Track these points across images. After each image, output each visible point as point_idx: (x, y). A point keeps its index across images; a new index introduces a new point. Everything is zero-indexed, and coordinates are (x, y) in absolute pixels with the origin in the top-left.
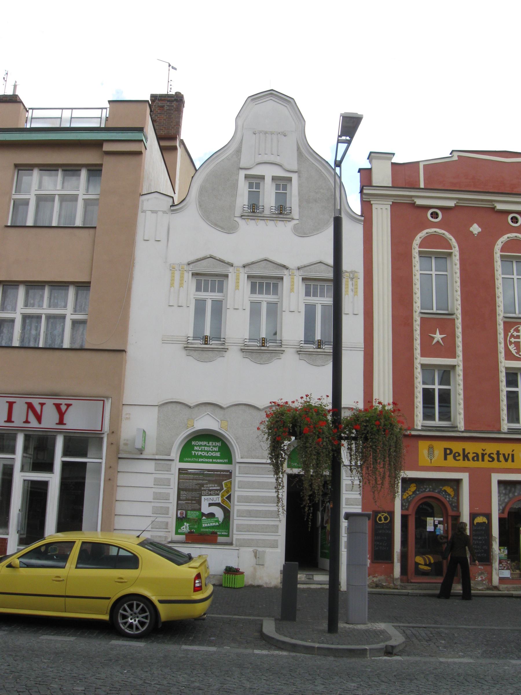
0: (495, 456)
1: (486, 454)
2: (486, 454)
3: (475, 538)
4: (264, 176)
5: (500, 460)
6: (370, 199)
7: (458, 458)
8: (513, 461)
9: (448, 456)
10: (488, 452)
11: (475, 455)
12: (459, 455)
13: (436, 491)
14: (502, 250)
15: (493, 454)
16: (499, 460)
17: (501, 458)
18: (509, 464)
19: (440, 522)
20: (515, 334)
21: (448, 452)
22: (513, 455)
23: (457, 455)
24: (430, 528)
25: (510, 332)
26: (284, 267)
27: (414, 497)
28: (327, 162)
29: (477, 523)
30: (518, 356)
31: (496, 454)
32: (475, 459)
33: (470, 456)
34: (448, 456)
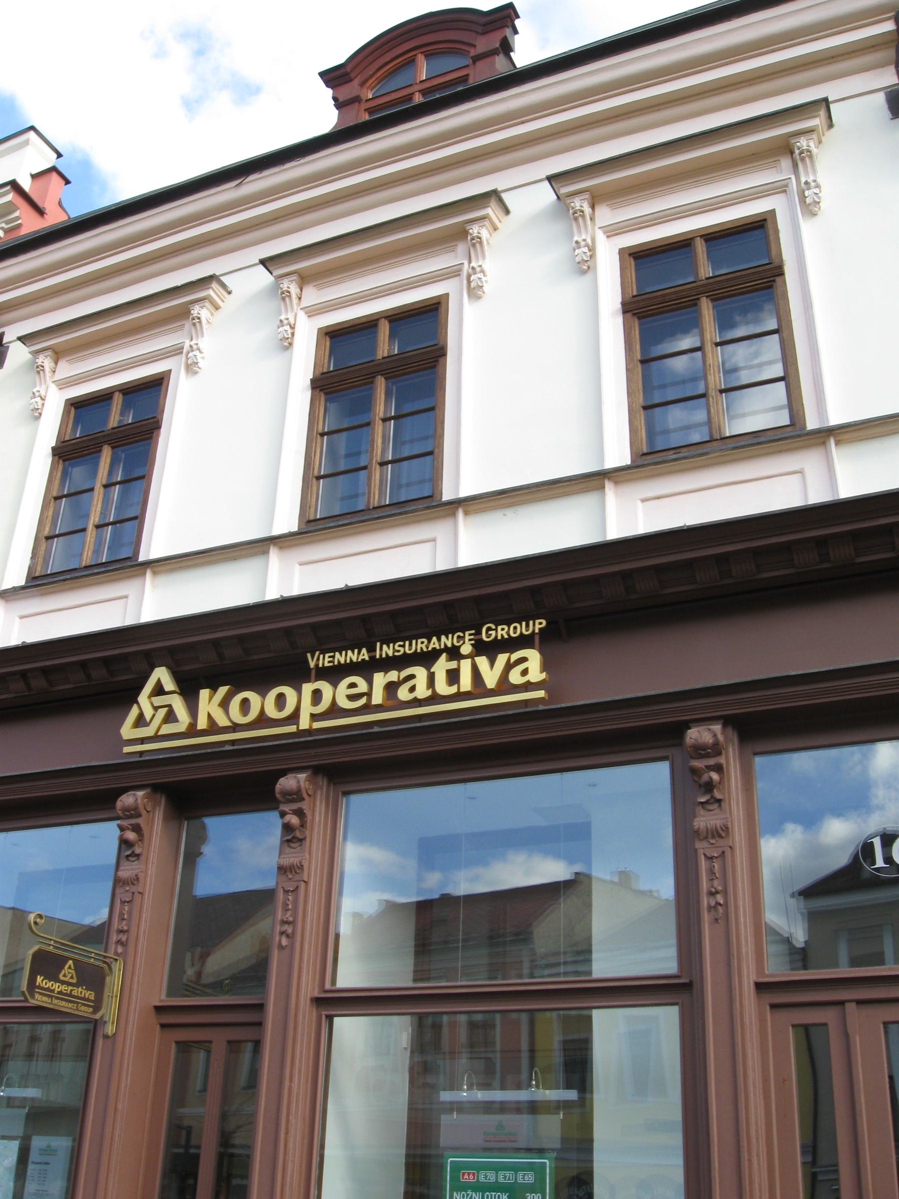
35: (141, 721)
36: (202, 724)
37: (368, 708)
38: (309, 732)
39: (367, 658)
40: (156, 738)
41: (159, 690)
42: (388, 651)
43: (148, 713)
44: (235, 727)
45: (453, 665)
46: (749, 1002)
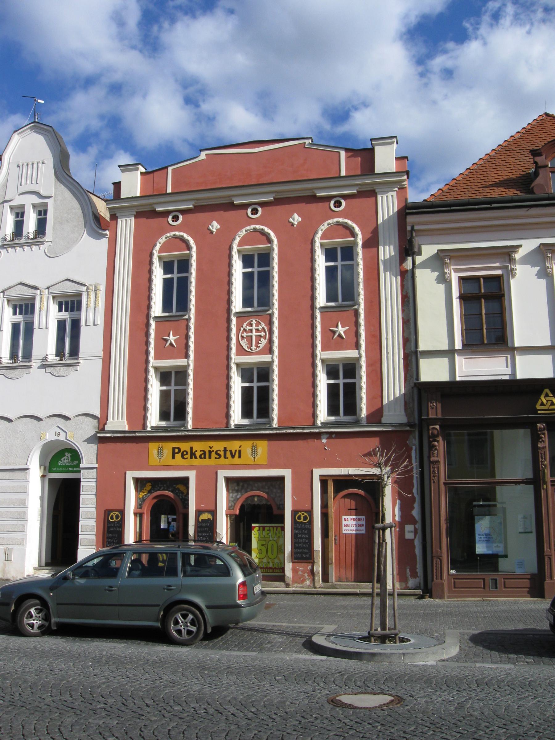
0: (222, 453)
1: (213, 451)
2: (213, 451)
3: (200, 534)
4: (25, 205)
5: (227, 456)
6: (116, 212)
7: (185, 457)
8: (240, 457)
9: (176, 455)
10: (215, 449)
11: (202, 452)
12: (187, 453)
13: (170, 490)
14: (240, 244)
15: (220, 451)
16: (225, 457)
17: (228, 454)
18: (236, 460)
19: (174, 520)
20: (248, 328)
21: (177, 450)
22: (240, 451)
23: (185, 453)
24: (163, 526)
25: (242, 327)
26: (36, 288)
27: (149, 496)
28: (78, 183)
29: (202, 520)
30: (250, 350)
31: (223, 451)
32: (203, 456)
33: (198, 454)
34: (176, 455)
35: (542, 404)
41: (547, 395)
43: (545, 401)
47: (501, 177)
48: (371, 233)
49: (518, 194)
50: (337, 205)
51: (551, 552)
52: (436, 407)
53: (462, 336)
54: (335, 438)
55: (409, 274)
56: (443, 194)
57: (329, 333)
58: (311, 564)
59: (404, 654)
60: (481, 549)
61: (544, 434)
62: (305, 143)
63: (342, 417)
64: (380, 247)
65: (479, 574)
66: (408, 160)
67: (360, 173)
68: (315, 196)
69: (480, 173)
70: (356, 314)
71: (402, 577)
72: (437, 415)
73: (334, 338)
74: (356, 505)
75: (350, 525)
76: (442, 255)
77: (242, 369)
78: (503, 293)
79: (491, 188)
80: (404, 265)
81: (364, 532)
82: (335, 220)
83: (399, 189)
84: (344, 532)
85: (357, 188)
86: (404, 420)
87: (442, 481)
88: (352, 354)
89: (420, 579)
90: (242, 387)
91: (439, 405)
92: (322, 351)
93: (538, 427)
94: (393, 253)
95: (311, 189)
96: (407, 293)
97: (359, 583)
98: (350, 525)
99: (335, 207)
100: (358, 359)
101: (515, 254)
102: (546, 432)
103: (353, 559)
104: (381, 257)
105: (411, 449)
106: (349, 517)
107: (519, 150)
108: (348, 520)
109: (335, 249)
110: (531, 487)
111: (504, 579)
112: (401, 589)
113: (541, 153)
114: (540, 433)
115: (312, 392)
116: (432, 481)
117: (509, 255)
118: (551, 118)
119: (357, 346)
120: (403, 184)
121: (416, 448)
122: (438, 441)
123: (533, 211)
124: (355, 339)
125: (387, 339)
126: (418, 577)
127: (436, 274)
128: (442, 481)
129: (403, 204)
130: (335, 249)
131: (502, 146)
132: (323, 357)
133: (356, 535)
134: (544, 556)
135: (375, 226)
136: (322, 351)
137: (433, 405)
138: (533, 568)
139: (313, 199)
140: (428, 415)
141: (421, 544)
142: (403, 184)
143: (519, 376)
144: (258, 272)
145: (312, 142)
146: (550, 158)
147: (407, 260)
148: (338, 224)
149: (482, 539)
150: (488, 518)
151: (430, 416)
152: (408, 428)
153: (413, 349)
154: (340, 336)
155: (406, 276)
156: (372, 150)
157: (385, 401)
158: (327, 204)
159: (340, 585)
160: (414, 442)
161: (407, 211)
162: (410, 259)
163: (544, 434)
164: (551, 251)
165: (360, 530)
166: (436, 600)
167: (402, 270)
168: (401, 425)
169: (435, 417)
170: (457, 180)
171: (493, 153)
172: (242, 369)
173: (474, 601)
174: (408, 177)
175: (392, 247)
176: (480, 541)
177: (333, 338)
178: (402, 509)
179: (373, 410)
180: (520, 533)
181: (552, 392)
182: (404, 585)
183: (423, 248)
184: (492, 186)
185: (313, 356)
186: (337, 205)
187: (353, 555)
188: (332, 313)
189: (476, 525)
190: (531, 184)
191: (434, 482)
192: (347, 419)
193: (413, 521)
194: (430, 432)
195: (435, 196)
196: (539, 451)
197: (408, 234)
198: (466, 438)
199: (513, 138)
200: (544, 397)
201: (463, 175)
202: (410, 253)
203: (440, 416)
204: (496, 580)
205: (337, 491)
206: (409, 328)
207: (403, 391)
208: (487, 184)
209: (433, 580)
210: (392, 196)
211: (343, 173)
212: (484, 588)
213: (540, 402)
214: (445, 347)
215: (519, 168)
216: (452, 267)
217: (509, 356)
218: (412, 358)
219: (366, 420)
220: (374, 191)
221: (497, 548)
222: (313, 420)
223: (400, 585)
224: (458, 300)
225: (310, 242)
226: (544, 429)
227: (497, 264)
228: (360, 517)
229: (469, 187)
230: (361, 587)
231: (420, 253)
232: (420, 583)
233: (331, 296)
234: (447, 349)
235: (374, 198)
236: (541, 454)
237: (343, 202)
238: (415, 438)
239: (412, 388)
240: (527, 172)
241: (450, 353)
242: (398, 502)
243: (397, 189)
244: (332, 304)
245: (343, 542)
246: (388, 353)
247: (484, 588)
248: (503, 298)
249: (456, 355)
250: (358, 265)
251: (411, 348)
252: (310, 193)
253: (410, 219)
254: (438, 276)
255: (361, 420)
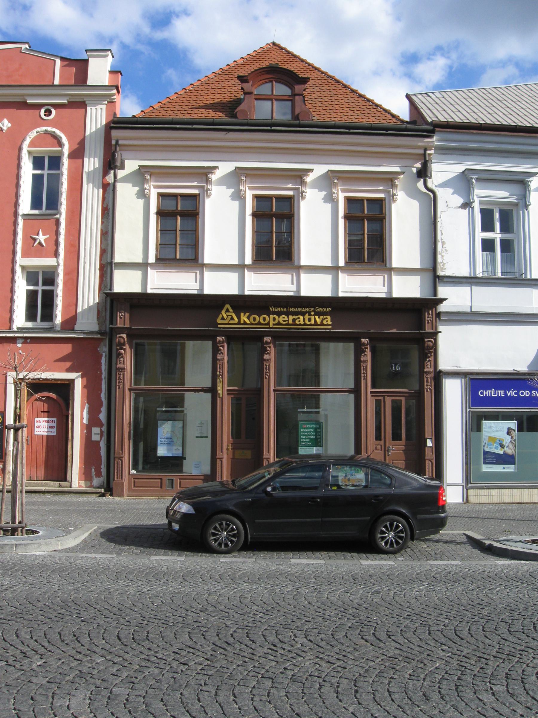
35: (223, 319)
36: (242, 322)
37: (288, 324)
38: (273, 328)
39: (286, 310)
40: (228, 324)
41: (227, 311)
42: (291, 309)
43: (225, 316)
44: (252, 324)
45: (310, 317)
46: (369, 395)
47: (213, 99)
48: (78, 144)
49: (223, 118)
50: (47, 113)
51: (222, 455)
52: (125, 316)
53: (157, 250)
54: (30, 343)
55: (111, 187)
56: (154, 111)
57: (30, 240)
58: (2, 463)
59: (16, 545)
60: (162, 451)
61: (223, 347)
62: (21, 48)
63: (39, 323)
64: (85, 158)
65: (159, 474)
66: (121, 75)
67: (73, 84)
68: (25, 103)
69: (194, 94)
70: (58, 222)
71: (86, 475)
72: (124, 325)
73: (35, 245)
74: (48, 408)
75: (42, 427)
76: (143, 170)
77: (27, 272)
78: (198, 211)
79: (199, 110)
80: (107, 178)
81: (55, 434)
82: (44, 128)
83: (108, 102)
84: (36, 433)
85: (68, 99)
86: (96, 328)
87: (127, 387)
88: (50, 261)
89: (103, 479)
90: (27, 290)
91: (127, 315)
92: (22, 258)
93: (218, 340)
94: (97, 166)
95: (23, 95)
96: (107, 206)
97: (47, 482)
98: (42, 427)
99: (45, 115)
100: (57, 267)
101: (212, 175)
102: (226, 345)
103: (44, 459)
104: (86, 169)
105: (101, 356)
106: (42, 419)
107: (232, 75)
108: (40, 422)
109: (43, 158)
110: (209, 396)
111: (180, 479)
112: (86, 487)
113: (248, 80)
114: (219, 345)
115: (10, 297)
116: (118, 387)
117: (207, 176)
118: (277, 48)
119: (56, 255)
120: (113, 98)
121: (106, 355)
122: (124, 350)
123: (232, 135)
124: (55, 247)
125: (85, 249)
126: (102, 476)
127: (137, 189)
128: (127, 387)
129: (111, 118)
130: (43, 158)
131: (223, 70)
132: (22, 264)
133: (47, 436)
134: (216, 459)
135: (83, 137)
136: (22, 258)
137: (122, 315)
138: (207, 469)
139: (23, 105)
140: (116, 324)
141: (106, 446)
142: (113, 98)
143: (206, 291)
144: (48, 174)
145: (30, 47)
146: (256, 86)
147: (110, 173)
148: (47, 133)
149: (164, 442)
150: (170, 422)
151: (118, 325)
152: (99, 336)
153: (109, 260)
154: (40, 244)
155: (108, 189)
156: (86, 61)
157: (80, 310)
158: (37, 111)
159: (30, 483)
160: (104, 350)
161: (112, 125)
162: (112, 172)
163: (223, 347)
164: (245, 175)
165: (51, 432)
166: (116, 498)
167: (105, 183)
168: (92, 332)
169: (123, 326)
170: (170, 99)
171: (213, 76)
172: (27, 272)
173: (150, 499)
174: (118, 92)
175: (96, 159)
176: (161, 444)
177: (33, 246)
178: (90, 412)
179: (68, 317)
180: (197, 437)
181: (233, 308)
182: (89, 483)
183: (127, 163)
184: (202, 107)
185: (13, 262)
186: (47, 113)
187: (44, 455)
188: (34, 221)
189: (159, 429)
190: (236, 109)
191: (119, 388)
192: (43, 325)
193: (100, 425)
194: (117, 340)
195: (145, 113)
196: (218, 362)
197: (113, 148)
198: (158, 347)
199: (236, 63)
200: (225, 312)
201: (178, 94)
202: (112, 166)
203: (127, 325)
204: (173, 480)
205: (29, 395)
206: (106, 240)
207: (97, 300)
208: (197, 105)
209: (114, 480)
210: (101, 109)
211: (57, 82)
212: (161, 487)
213: (220, 316)
214: (140, 260)
215: (232, 93)
216: (152, 183)
217: (198, 272)
218: (107, 269)
219: (60, 327)
220: (84, 102)
221: (177, 451)
222: (9, 324)
223: (85, 484)
224: (156, 216)
225: (18, 148)
226: (223, 342)
227: (195, 184)
228: (52, 419)
229: (180, 107)
230: (48, 486)
231: (122, 167)
232: (103, 482)
233: (36, 203)
234: (141, 262)
235: (84, 110)
236: (220, 365)
237: (53, 111)
238: (105, 346)
239: (106, 297)
240: (238, 97)
241: (143, 266)
242: (87, 405)
243: (106, 102)
244: (36, 212)
245: (35, 443)
246: (85, 263)
247: (161, 487)
248: (197, 217)
249: (149, 268)
250: (62, 175)
251: (107, 259)
252: (22, 99)
253: (115, 133)
254: (138, 191)
255: (56, 327)
